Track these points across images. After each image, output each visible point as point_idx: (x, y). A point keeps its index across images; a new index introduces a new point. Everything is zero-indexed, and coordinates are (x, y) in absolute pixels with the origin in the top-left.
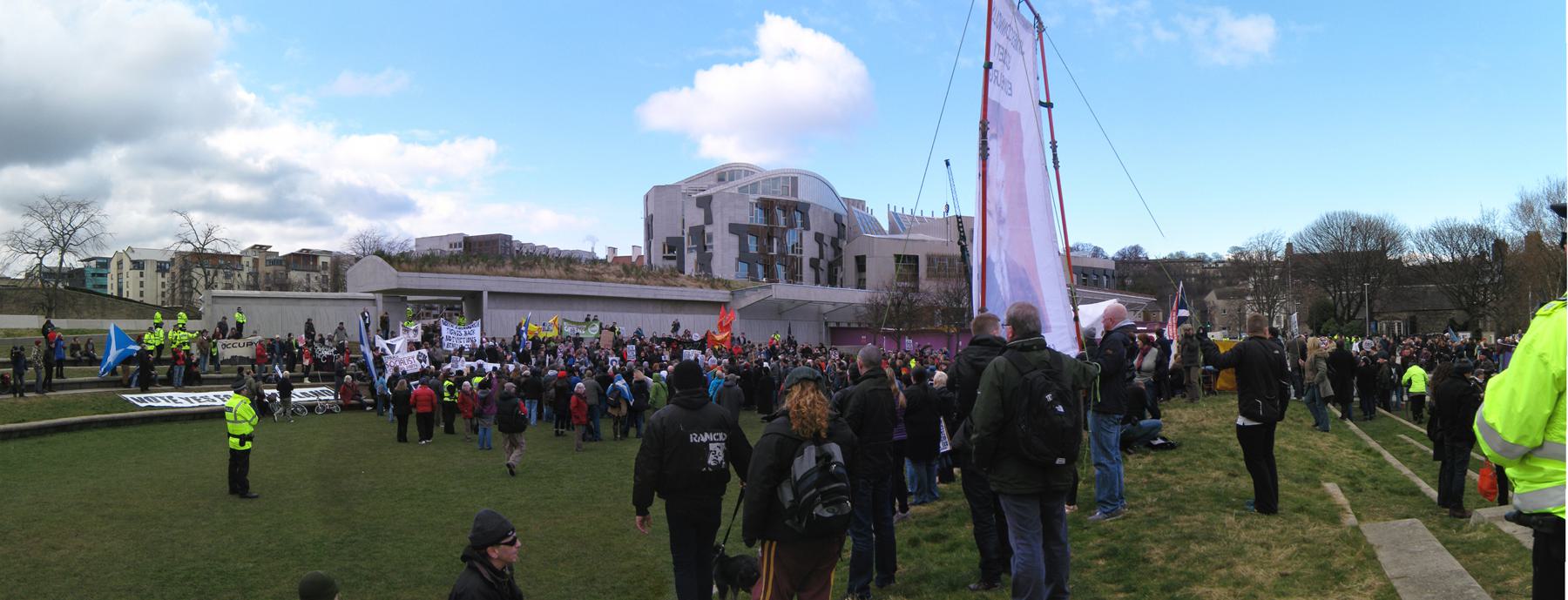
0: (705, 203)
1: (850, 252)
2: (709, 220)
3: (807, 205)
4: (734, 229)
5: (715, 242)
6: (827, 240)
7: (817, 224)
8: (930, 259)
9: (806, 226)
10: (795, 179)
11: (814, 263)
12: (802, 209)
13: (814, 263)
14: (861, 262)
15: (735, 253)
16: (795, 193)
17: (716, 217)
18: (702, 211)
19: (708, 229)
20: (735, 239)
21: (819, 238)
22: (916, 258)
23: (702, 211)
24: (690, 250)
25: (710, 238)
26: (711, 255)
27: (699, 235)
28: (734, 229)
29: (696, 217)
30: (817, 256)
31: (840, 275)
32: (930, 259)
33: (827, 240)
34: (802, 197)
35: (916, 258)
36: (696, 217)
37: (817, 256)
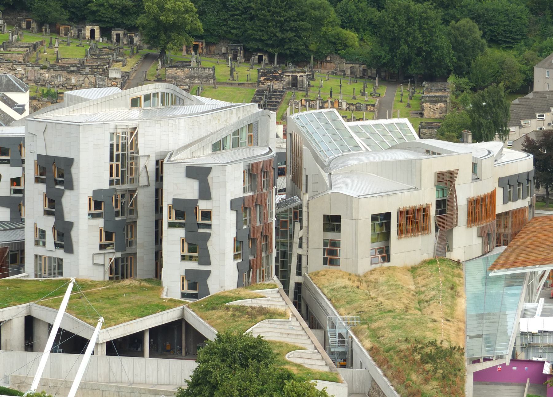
0: (199, 174)
2: (205, 193)
4: (235, 204)
5: (214, 221)
14: (333, 223)
15: (232, 233)
17: (214, 193)
18: (194, 185)
23: (194, 185)
24: (171, 225)
25: (207, 215)
26: (210, 234)
28: (235, 204)
29: (189, 190)
31: (298, 233)
36: (189, 190)
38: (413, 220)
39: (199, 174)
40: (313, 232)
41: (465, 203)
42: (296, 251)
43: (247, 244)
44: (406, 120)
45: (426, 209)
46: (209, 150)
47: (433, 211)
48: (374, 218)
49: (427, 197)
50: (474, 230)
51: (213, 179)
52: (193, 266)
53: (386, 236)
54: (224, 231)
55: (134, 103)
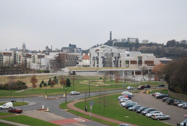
1: (119, 60)
2: (98, 56)
3: (113, 53)
4: (102, 57)
6: (117, 58)
7: (115, 55)
8: (131, 61)
9: (113, 56)
10: (111, 49)
11: (114, 61)
12: (112, 54)
13: (114, 61)
14: (121, 61)
15: (102, 61)
16: (111, 51)
17: (99, 56)
19: (98, 57)
20: (102, 59)
21: (115, 58)
22: (129, 61)
27: (97, 58)
28: (102, 57)
29: (97, 55)
30: (115, 60)
32: (131, 61)
33: (117, 58)
34: (113, 52)
35: (129, 61)
36: (97, 55)
37: (115, 60)
38: (133, 62)
39: (98, 53)
40: (119, 62)
41: (144, 61)
42: (118, 65)
43: (104, 62)
44: (153, 54)
45: (136, 61)
46: (102, 52)
47: (138, 61)
48: (126, 61)
49: (137, 60)
50: (146, 65)
51: (99, 54)
52: (97, 65)
53: (129, 64)
54: (101, 60)
55: (102, 47)
